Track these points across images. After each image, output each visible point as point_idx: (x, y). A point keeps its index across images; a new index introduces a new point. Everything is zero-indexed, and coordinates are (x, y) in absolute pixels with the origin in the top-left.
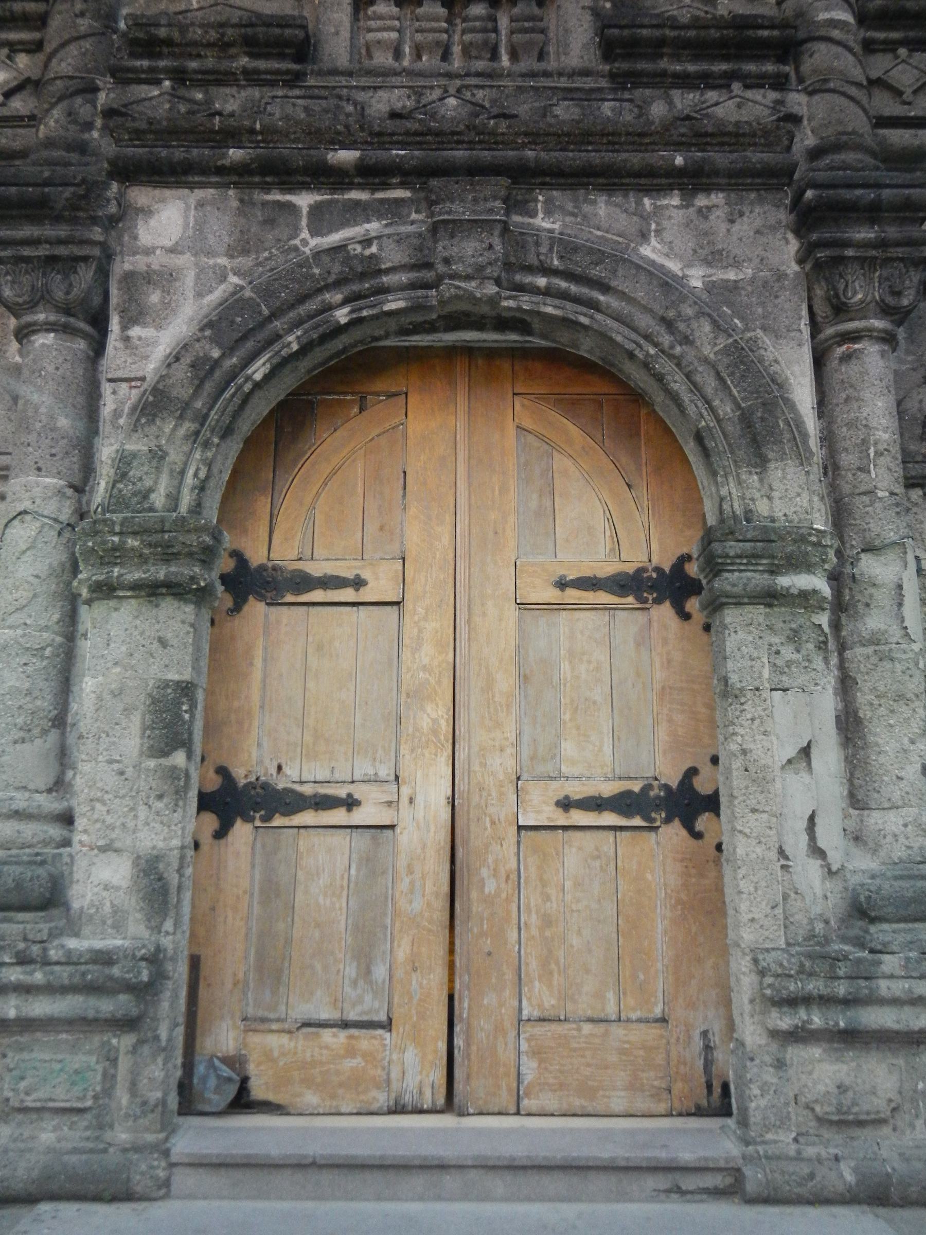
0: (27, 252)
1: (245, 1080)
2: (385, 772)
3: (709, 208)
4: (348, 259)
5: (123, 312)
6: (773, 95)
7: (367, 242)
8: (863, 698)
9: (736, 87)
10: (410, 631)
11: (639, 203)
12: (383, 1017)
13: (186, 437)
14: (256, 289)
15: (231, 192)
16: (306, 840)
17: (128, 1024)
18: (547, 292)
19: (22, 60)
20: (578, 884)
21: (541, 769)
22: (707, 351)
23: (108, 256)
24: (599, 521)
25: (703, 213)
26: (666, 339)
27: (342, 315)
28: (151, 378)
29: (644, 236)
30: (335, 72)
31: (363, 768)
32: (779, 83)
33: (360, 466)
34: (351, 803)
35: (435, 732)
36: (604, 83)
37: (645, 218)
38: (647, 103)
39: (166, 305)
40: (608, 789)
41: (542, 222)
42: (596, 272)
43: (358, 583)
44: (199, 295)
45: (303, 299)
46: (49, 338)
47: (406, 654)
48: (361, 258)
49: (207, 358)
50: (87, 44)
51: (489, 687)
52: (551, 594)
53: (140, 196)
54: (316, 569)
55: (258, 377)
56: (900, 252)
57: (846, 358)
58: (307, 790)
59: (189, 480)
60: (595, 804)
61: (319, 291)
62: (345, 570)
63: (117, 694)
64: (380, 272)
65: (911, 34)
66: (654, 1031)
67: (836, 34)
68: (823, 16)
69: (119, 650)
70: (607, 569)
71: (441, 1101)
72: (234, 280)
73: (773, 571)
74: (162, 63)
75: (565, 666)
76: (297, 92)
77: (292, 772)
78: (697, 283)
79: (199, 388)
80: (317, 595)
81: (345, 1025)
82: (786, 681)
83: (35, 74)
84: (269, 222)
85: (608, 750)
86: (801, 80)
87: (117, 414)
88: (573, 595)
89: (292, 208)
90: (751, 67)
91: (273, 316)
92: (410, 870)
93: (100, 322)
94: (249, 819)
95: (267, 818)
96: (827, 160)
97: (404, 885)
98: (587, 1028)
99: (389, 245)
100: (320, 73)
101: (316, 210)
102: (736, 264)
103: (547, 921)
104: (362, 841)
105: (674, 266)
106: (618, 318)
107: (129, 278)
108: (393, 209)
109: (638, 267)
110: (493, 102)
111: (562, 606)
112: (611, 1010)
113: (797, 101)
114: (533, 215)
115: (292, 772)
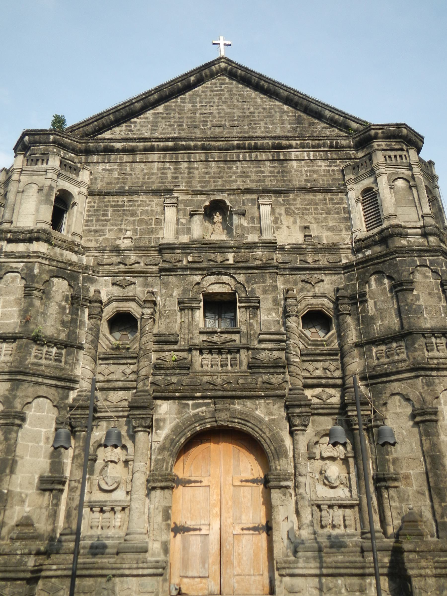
0: (138, 416)
1: (180, 588)
2: (207, 523)
3: (269, 403)
4: (200, 416)
5: (155, 427)
6: (283, 376)
7: (203, 413)
8: (299, 506)
9: (275, 375)
10: (211, 492)
11: (255, 402)
12: (207, 575)
13: (169, 456)
14: (181, 423)
15: (176, 401)
16: (192, 538)
17: (161, 575)
18: (238, 423)
19: (132, 366)
20: (245, 546)
21: (238, 521)
22: (268, 435)
23: (153, 415)
24: (249, 467)
25: (268, 404)
26: (260, 432)
27: (198, 429)
28: (161, 443)
29: (256, 409)
30: (196, 372)
31: (203, 522)
32: (284, 373)
33: (201, 456)
34: (200, 530)
35: (217, 514)
36: (249, 373)
37: (256, 405)
38: (258, 378)
39: (164, 426)
40: (251, 526)
41: (237, 407)
42: (247, 419)
43: (201, 482)
44: (170, 423)
45: (190, 425)
46: (142, 433)
47: (211, 497)
48: (202, 416)
49: (173, 438)
50: (147, 368)
51: (227, 503)
52: (239, 483)
53: (158, 402)
54: (193, 479)
55: (182, 442)
56: (305, 414)
57: (296, 434)
58: (191, 527)
59: (170, 464)
60: (248, 529)
61: (194, 423)
62: (198, 479)
63: (158, 508)
64: (205, 419)
65: (312, 358)
66: (261, 577)
67: (295, 364)
68: (292, 360)
69: (157, 500)
70: (251, 477)
71: (219, 592)
72: (177, 420)
73: (280, 481)
74: (162, 372)
75: (242, 499)
76: (189, 377)
77: (188, 523)
78: (267, 419)
79: (171, 445)
80: (193, 484)
81: (200, 577)
82: (283, 503)
83: (135, 370)
84: (184, 407)
85: (251, 517)
86: (289, 372)
87: (155, 449)
88: (244, 483)
89: (188, 405)
90: (278, 371)
91: (185, 429)
92: (212, 544)
93: (150, 427)
94: (180, 533)
95: (184, 533)
96: (292, 392)
97: (211, 547)
98: (247, 577)
99: (207, 413)
100: (193, 373)
101: (193, 405)
102: (275, 415)
103: (239, 554)
104: (203, 538)
105: (262, 416)
106: (251, 428)
107: (157, 420)
108: (208, 405)
109: (255, 418)
110: (227, 379)
111: (242, 486)
112: (252, 573)
113: (288, 377)
114: (235, 405)
115: (188, 523)
